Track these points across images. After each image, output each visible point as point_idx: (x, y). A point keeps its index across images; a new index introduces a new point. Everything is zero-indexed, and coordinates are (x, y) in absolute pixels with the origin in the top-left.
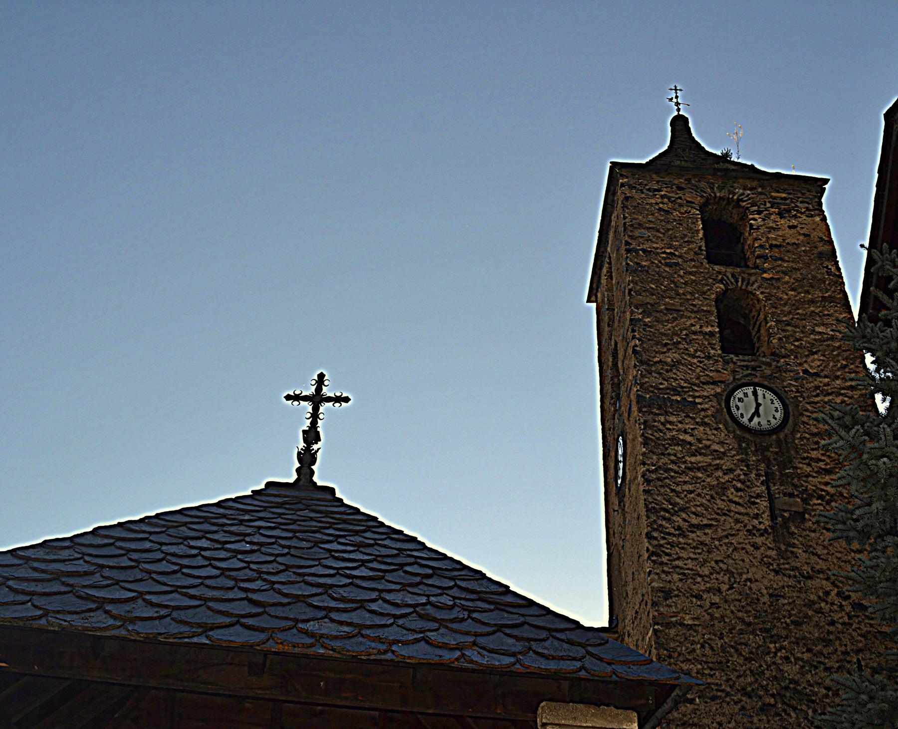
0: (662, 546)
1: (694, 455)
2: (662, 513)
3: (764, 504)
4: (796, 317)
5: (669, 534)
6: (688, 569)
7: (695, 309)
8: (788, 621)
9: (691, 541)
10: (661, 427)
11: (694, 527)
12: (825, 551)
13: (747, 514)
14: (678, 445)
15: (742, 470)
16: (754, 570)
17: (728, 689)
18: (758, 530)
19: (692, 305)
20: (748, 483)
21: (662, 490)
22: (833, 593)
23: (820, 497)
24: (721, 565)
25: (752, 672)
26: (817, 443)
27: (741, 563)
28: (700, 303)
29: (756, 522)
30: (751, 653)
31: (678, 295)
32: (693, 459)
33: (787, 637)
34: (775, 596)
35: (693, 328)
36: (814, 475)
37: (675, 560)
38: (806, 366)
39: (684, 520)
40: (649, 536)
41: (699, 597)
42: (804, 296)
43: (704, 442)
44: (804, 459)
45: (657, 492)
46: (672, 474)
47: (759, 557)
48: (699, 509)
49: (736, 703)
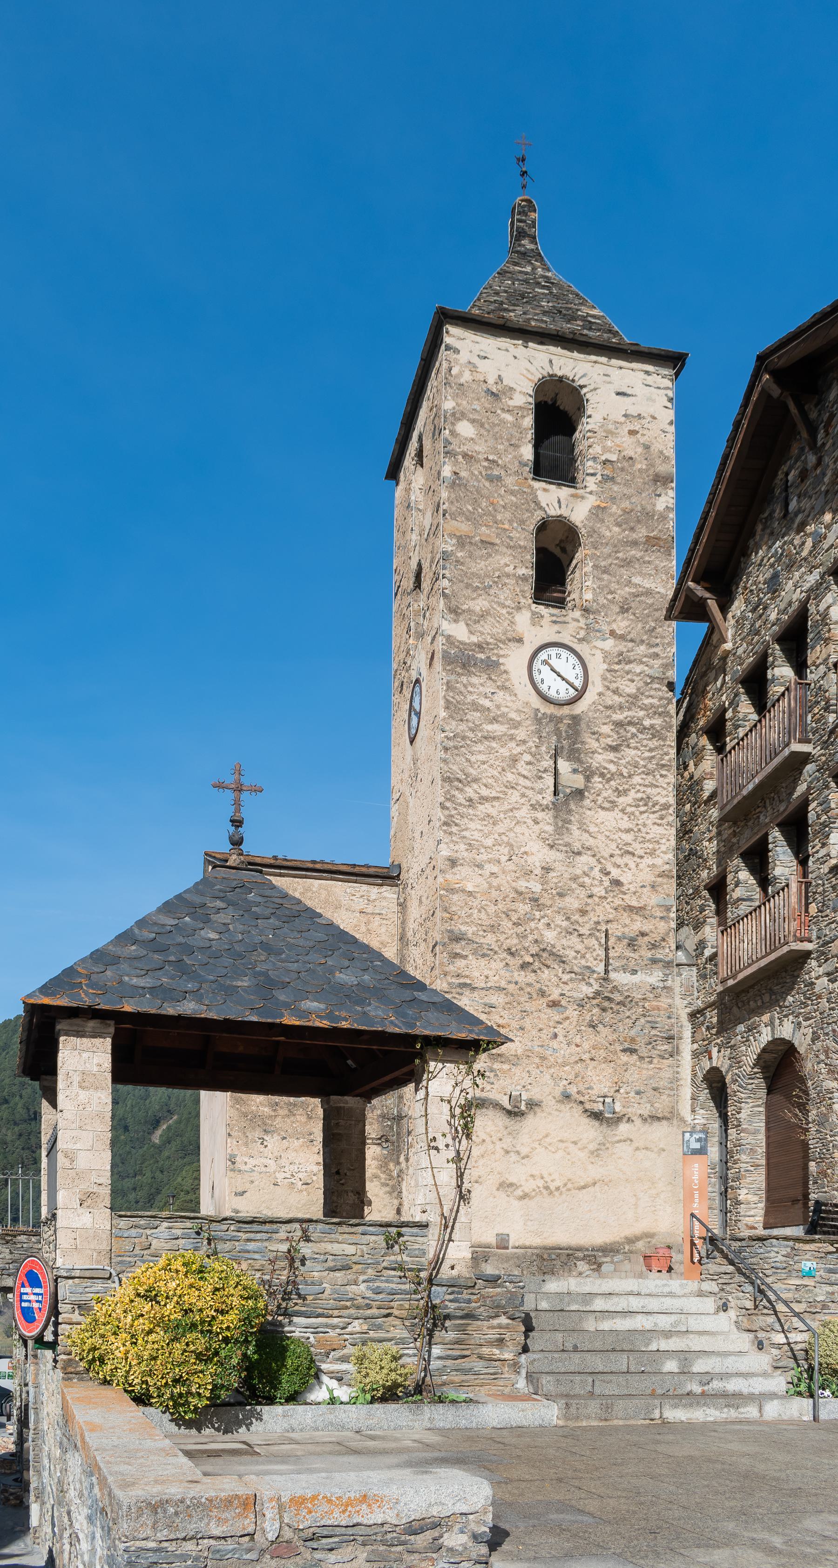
0: (452, 816)
1: (491, 723)
2: (456, 783)
3: (549, 781)
4: (615, 562)
5: (461, 805)
7: (512, 544)
8: (554, 892)
9: (479, 813)
10: (463, 689)
11: (484, 799)
12: (596, 829)
14: (477, 710)
15: (534, 742)
16: (531, 844)
17: (497, 949)
18: (541, 805)
19: (509, 537)
20: (538, 757)
21: (458, 759)
22: (597, 869)
23: (602, 775)
24: (503, 837)
25: (517, 935)
26: (608, 717)
27: (521, 836)
28: (518, 535)
29: (540, 797)
30: (519, 919)
31: (496, 523)
32: (490, 727)
33: (551, 906)
34: (547, 869)
35: (507, 569)
36: (600, 751)
37: (463, 830)
38: (614, 626)
39: (476, 792)
40: (443, 807)
41: (480, 866)
43: (502, 709)
44: (594, 733)
45: (453, 761)
46: (469, 742)
47: (538, 831)
48: (490, 781)
49: (502, 960)
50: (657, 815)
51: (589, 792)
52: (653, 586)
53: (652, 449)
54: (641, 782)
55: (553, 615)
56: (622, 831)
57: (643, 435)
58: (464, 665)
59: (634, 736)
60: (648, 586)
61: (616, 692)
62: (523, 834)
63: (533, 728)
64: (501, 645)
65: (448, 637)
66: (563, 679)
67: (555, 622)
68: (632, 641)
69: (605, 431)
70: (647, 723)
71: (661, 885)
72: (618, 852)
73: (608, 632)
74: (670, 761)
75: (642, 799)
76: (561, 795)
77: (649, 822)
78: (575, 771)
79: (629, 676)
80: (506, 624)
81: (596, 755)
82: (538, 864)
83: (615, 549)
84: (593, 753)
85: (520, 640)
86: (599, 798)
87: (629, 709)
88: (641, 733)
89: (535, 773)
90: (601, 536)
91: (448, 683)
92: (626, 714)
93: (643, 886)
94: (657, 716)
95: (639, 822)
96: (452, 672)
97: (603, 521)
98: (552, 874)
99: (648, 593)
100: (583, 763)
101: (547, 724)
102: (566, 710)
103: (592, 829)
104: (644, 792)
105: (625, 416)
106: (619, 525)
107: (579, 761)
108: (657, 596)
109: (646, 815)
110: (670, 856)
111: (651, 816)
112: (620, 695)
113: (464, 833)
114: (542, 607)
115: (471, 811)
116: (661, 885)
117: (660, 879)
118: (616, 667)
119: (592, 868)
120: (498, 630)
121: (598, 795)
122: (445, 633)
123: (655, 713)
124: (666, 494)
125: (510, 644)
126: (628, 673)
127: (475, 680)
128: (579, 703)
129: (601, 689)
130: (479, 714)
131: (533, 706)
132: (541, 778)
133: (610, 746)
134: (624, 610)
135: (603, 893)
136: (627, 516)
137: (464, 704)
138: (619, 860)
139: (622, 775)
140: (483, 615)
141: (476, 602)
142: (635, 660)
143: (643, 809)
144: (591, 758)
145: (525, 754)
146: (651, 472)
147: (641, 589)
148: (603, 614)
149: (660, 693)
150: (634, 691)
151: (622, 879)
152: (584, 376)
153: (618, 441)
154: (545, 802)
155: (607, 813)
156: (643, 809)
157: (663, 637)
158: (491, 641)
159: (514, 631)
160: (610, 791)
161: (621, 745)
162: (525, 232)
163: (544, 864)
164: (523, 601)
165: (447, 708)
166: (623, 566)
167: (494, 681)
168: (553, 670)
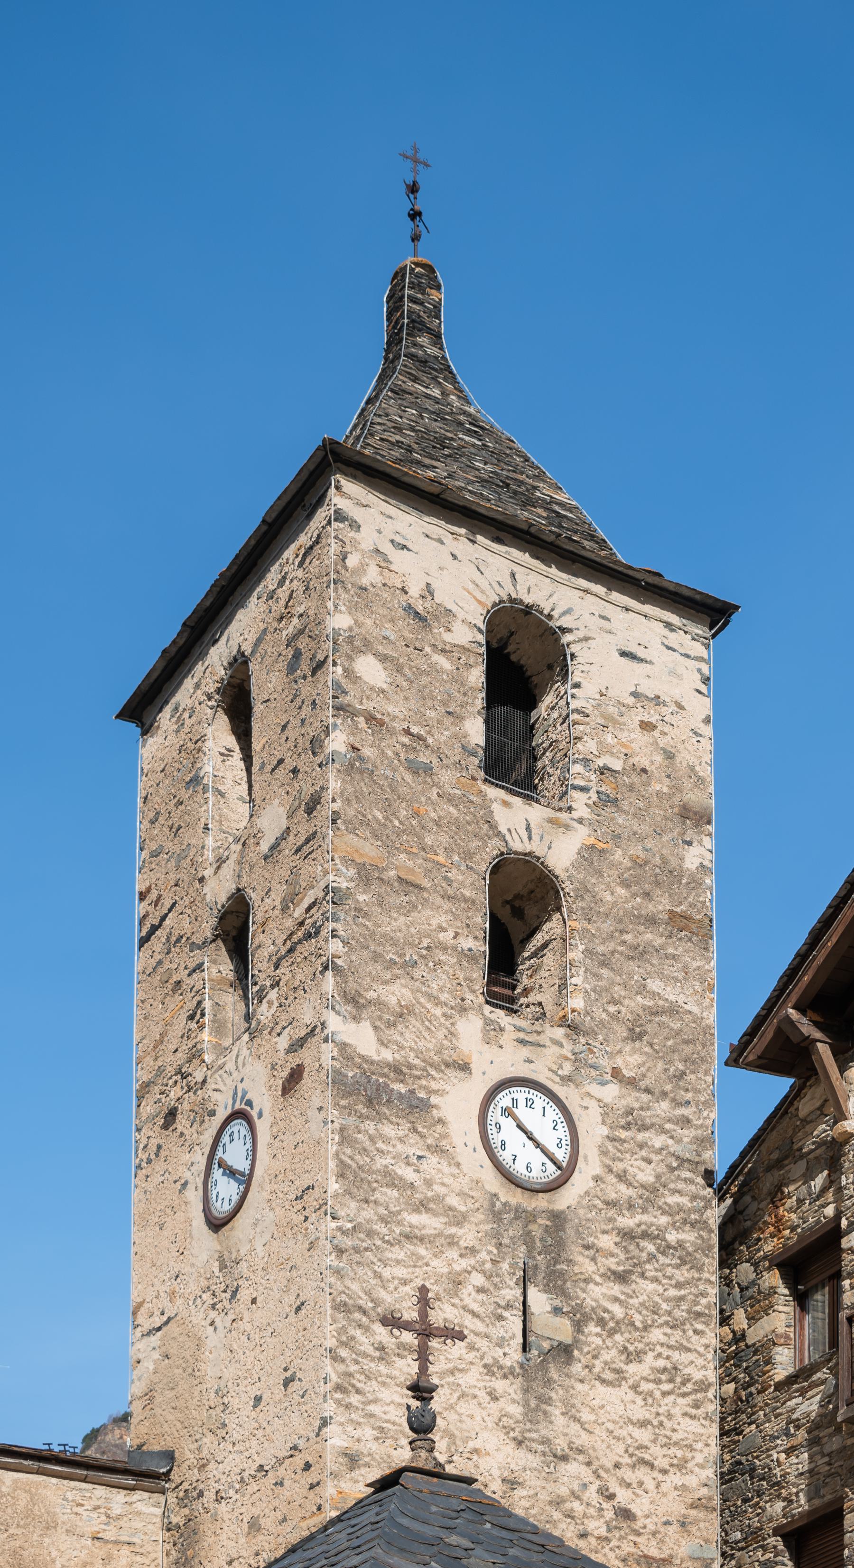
0: (350, 1375)
1: (416, 1210)
2: (357, 1315)
3: (515, 1324)
4: (620, 948)
5: (365, 1355)
6: (387, 1421)
7: (450, 892)
9: (396, 1373)
10: (368, 1144)
12: (592, 1417)
13: (487, 1336)
18: (501, 1367)
20: (496, 1280)
21: (360, 1271)
22: (593, 1488)
23: (601, 1322)
26: (611, 1220)
27: (468, 1420)
29: (500, 1352)
32: (414, 1219)
35: (441, 935)
36: (598, 1279)
37: (370, 1402)
38: (619, 1062)
42: (640, 905)
43: (435, 1187)
44: (587, 1247)
45: (352, 1275)
46: (379, 1242)
47: (497, 1414)
50: (689, 1400)
51: (580, 1350)
52: (681, 999)
53: (678, 760)
54: (663, 1339)
55: (519, 1029)
56: (633, 1424)
57: (663, 733)
58: (370, 1101)
59: (651, 1257)
60: (672, 998)
61: (622, 1177)
62: (472, 1417)
63: (488, 1227)
64: (433, 1073)
65: (343, 1047)
66: (538, 1145)
67: (522, 1042)
68: (647, 1091)
69: (602, 716)
70: (672, 1237)
71: (696, 1522)
72: (627, 1460)
73: (609, 1070)
74: (708, 1306)
75: (664, 1370)
76: (535, 1352)
77: (677, 1411)
78: (557, 1311)
79: (644, 1153)
80: (441, 1034)
81: (591, 1286)
82: (496, 1473)
83: (620, 927)
84: (587, 1281)
85: (464, 1067)
86: (597, 1362)
87: (644, 1211)
88: (663, 1253)
89: (492, 1308)
90: (598, 901)
91: (342, 1130)
92: (639, 1218)
93: (667, 1523)
94: (687, 1227)
95: (661, 1411)
96: (349, 1110)
97: (599, 873)
98: (520, 1492)
99: (673, 1010)
100: (570, 1298)
101: (511, 1223)
102: (541, 1202)
103: (586, 1416)
104: (668, 1358)
105: (635, 694)
106: (626, 884)
107: (563, 1293)
108: (688, 1017)
109: (671, 1398)
110: (710, 1473)
111: (681, 1401)
112: (630, 1185)
113: (372, 1408)
114: (500, 1013)
115: (382, 1368)
116: (696, 1522)
117: (693, 1512)
118: (623, 1134)
119: (585, 1486)
120: (428, 1044)
121: (595, 1357)
122: (338, 1038)
123: (685, 1221)
124: (700, 842)
125: (448, 1071)
126: (642, 1146)
127: (388, 1130)
128: (563, 1191)
129: (598, 1170)
130: (395, 1193)
131: (488, 1187)
132: (500, 1318)
133: (614, 1273)
134: (635, 1035)
135: (603, 1531)
136: (638, 871)
137: (370, 1172)
138: (628, 1475)
139: (632, 1324)
140: (403, 1014)
141: (391, 988)
142: (653, 1125)
143: (666, 1387)
144: (584, 1291)
145: (474, 1273)
146: (676, 800)
147: (661, 1003)
148: (600, 1037)
149: (693, 1188)
150: (652, 1179)
151: (634, 1508)
152: (568, 612)
153: (623, 736)
154: (507, 1362)
155: (610, 1390)
156: (666, 1387)
157: (697, 1091)
158: (417, 1062)
159: (454, 1049)
160: (614, 1352)
161: (630, 1272)
162: (422, 323)
163: (506, 1474)
164: (469, 996)
165: (341, 1176)
166: (633, 958)
167: (423, 1136)
168: (520, 1127)
